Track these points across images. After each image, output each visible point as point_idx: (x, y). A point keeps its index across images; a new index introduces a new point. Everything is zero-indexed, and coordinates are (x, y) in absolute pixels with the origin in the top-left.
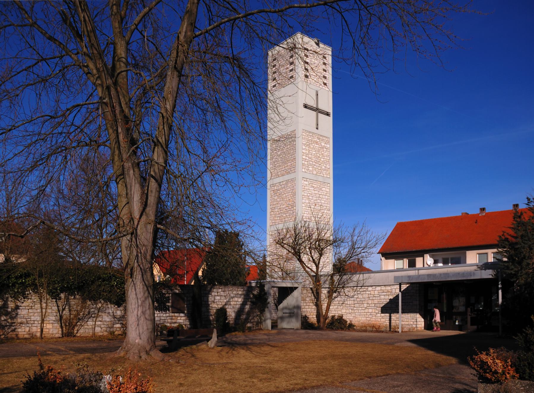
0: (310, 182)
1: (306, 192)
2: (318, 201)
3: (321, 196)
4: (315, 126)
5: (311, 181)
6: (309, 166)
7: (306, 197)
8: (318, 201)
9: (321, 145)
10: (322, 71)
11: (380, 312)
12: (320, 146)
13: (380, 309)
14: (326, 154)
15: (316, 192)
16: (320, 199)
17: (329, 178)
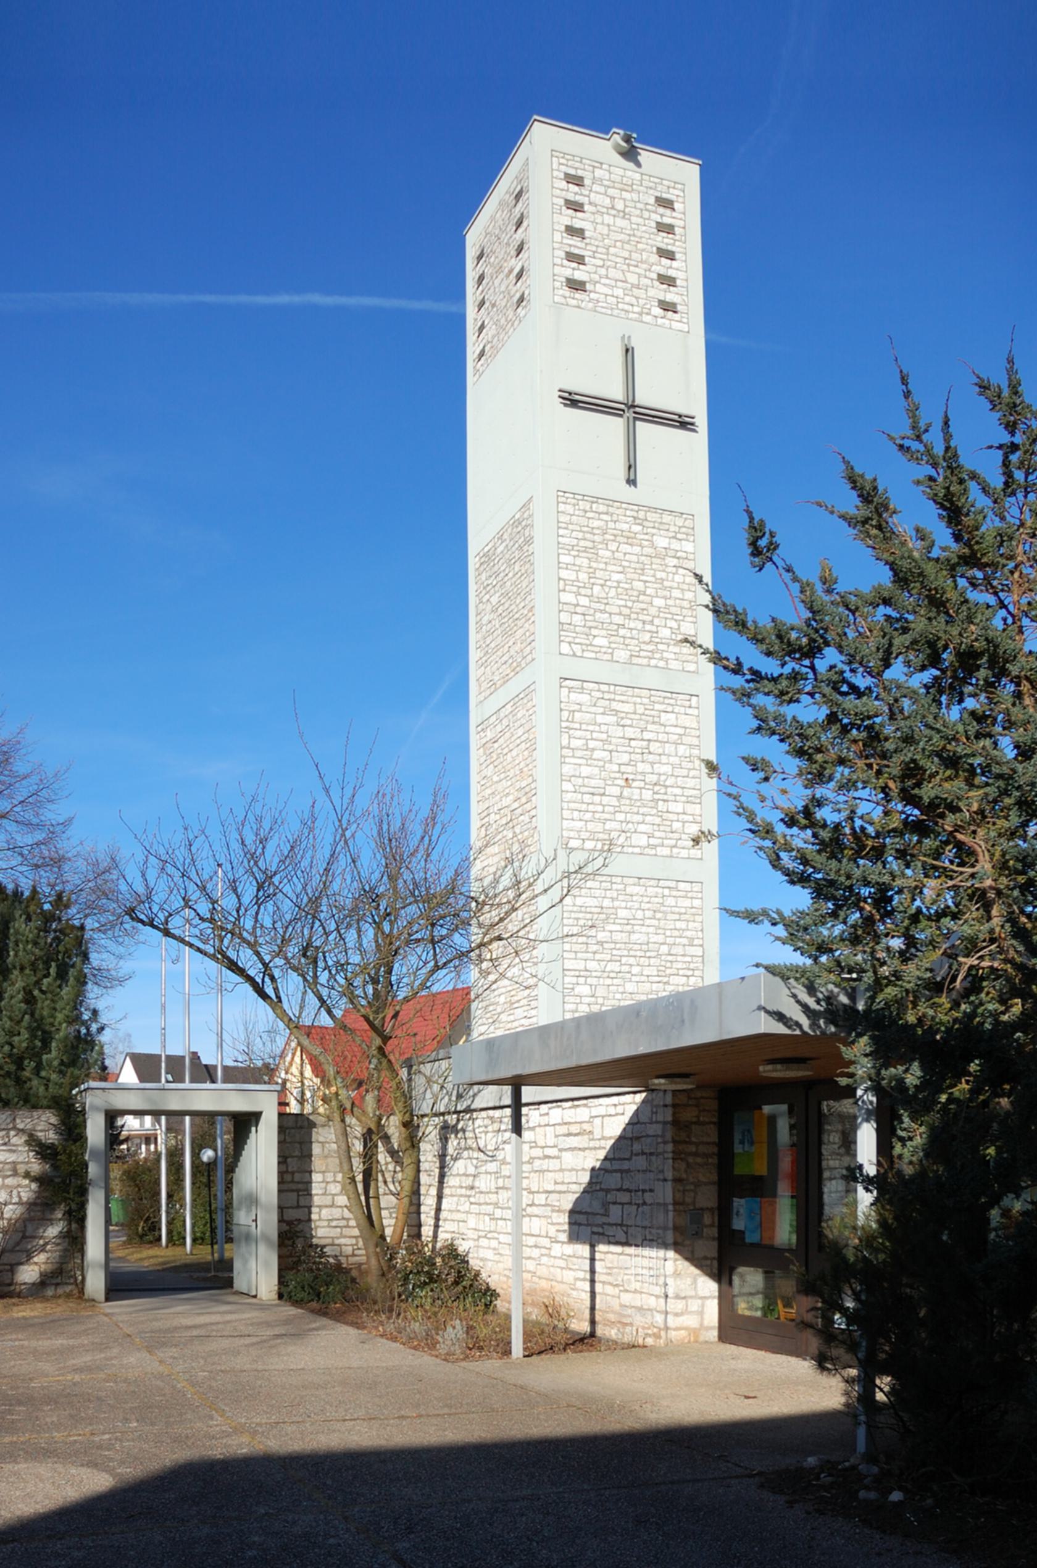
0: (599, 695)
1: (578, 733)
2: (641, 767)
3: (654, 747)
4: (621, 473)
5: (604, 688)
6: (594, 632)
7: (579, 753)
8: (641, 767)
9: (653, 546)
10: (654, 258)
11: (564, 1237)
12: (647, 551)
13: (564, 1218)
14: (678, 578)
15: (630, 732)
16: (651, 758)
17: (696, 672)
